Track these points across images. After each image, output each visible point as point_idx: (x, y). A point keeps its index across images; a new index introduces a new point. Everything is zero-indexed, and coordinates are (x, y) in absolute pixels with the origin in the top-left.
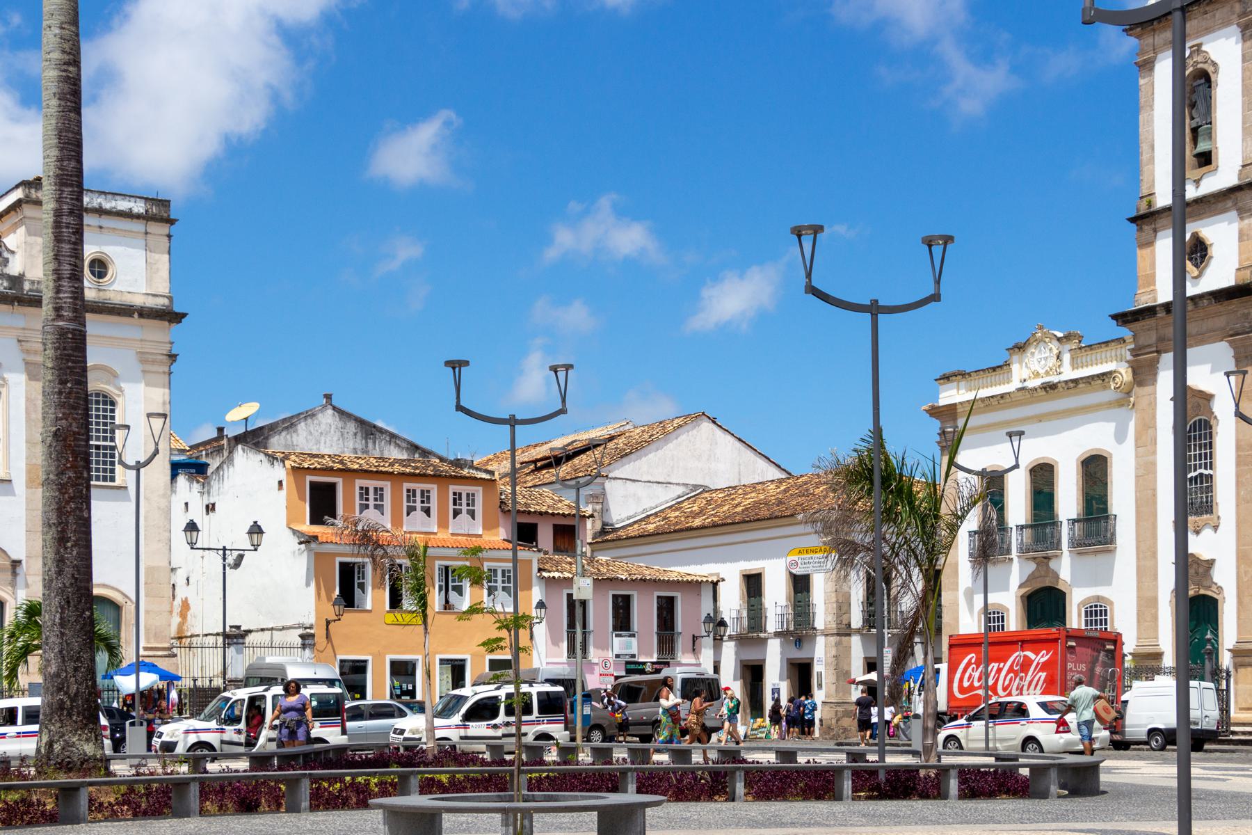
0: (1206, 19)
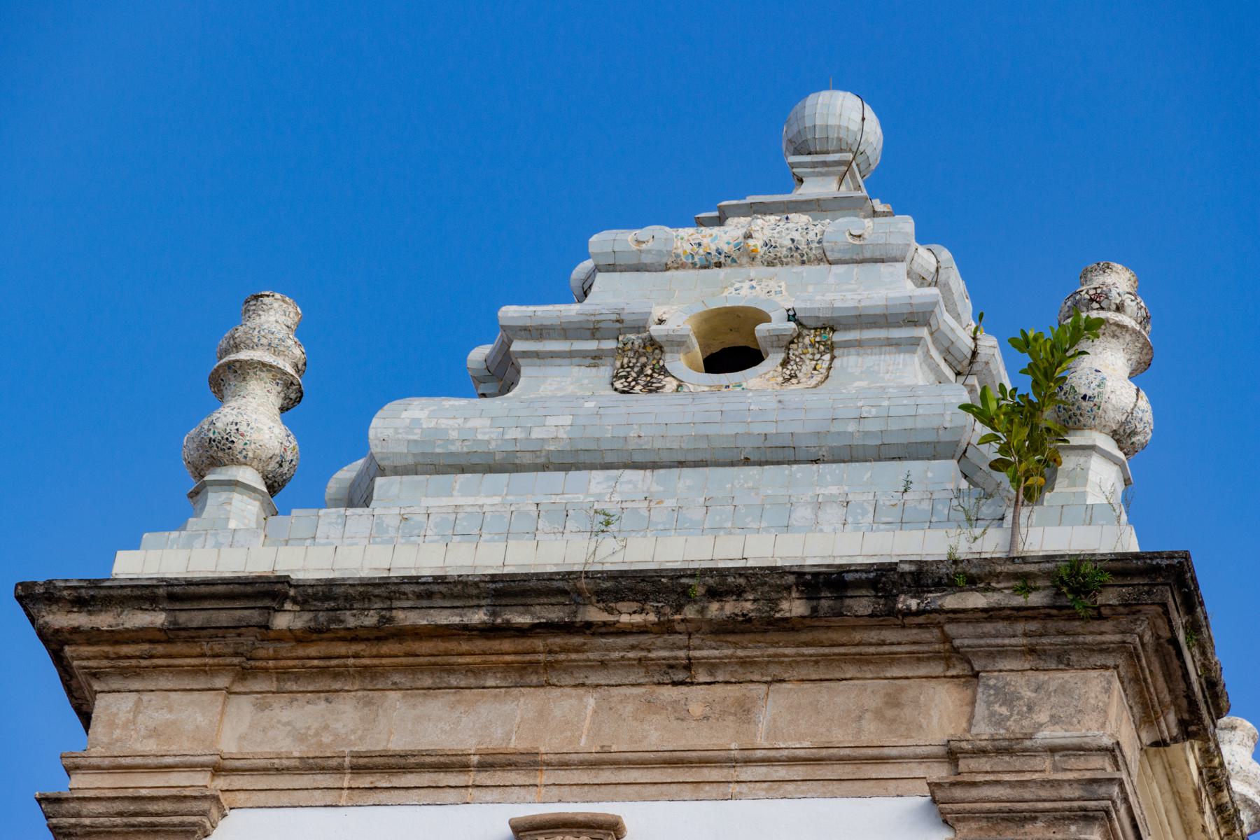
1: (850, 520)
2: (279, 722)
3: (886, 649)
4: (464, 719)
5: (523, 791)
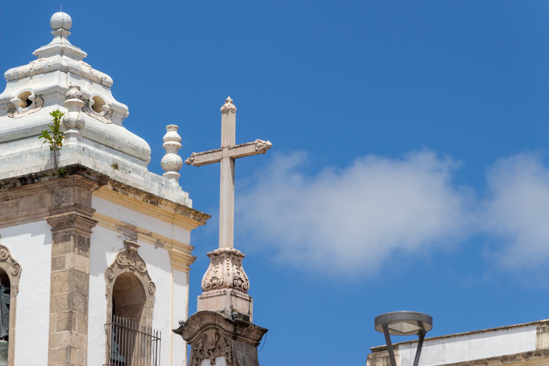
1: (32, 157)
3: (37, 189)
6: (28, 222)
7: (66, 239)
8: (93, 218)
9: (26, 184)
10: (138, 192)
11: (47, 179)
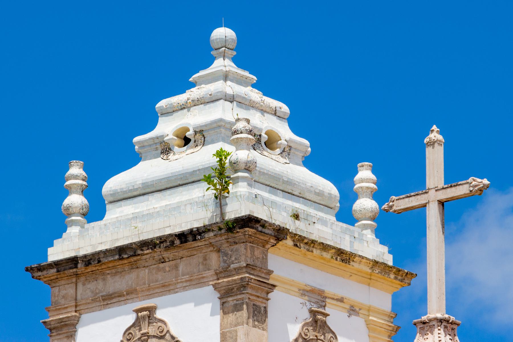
0: (164, 269)
1: (192, 208)
2: (88, 288)
3: (200, 247)
4: (123, 281)
5: (136, 299)
6: (190, 289)
7: (237, 308)
8: (271, 282)
9: (186, 241)
10: (325, 247)
11: (211, 234)
